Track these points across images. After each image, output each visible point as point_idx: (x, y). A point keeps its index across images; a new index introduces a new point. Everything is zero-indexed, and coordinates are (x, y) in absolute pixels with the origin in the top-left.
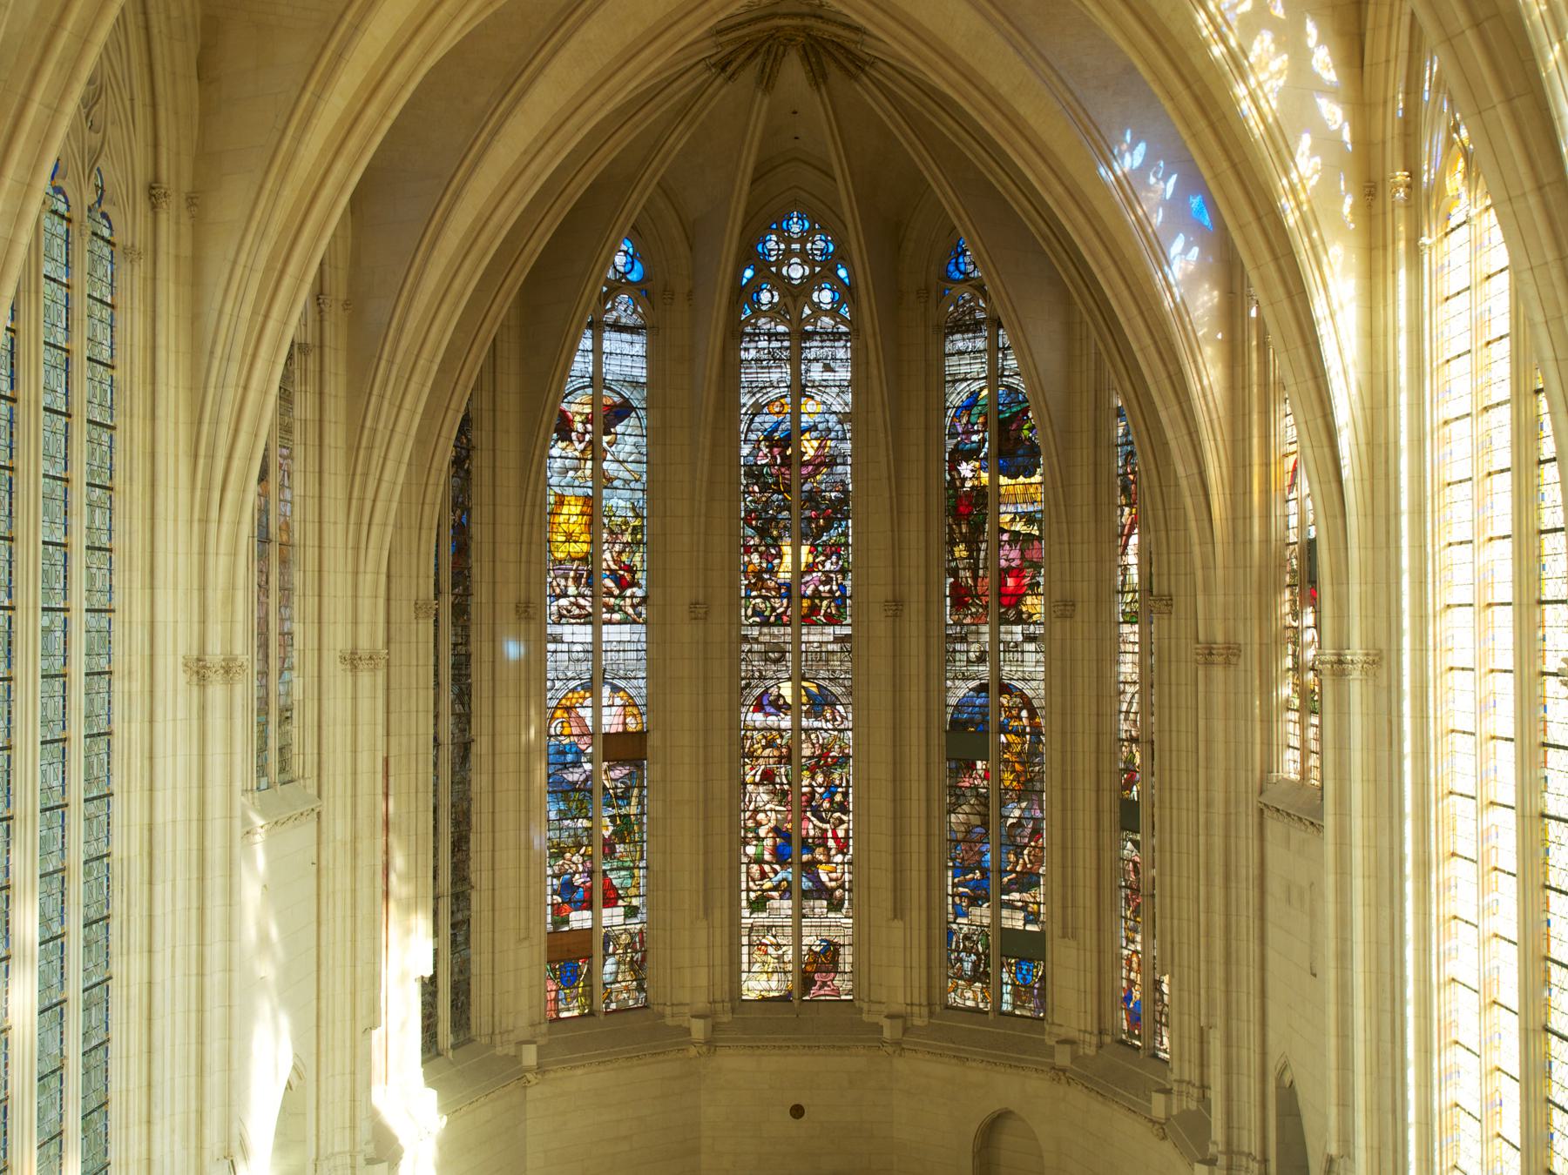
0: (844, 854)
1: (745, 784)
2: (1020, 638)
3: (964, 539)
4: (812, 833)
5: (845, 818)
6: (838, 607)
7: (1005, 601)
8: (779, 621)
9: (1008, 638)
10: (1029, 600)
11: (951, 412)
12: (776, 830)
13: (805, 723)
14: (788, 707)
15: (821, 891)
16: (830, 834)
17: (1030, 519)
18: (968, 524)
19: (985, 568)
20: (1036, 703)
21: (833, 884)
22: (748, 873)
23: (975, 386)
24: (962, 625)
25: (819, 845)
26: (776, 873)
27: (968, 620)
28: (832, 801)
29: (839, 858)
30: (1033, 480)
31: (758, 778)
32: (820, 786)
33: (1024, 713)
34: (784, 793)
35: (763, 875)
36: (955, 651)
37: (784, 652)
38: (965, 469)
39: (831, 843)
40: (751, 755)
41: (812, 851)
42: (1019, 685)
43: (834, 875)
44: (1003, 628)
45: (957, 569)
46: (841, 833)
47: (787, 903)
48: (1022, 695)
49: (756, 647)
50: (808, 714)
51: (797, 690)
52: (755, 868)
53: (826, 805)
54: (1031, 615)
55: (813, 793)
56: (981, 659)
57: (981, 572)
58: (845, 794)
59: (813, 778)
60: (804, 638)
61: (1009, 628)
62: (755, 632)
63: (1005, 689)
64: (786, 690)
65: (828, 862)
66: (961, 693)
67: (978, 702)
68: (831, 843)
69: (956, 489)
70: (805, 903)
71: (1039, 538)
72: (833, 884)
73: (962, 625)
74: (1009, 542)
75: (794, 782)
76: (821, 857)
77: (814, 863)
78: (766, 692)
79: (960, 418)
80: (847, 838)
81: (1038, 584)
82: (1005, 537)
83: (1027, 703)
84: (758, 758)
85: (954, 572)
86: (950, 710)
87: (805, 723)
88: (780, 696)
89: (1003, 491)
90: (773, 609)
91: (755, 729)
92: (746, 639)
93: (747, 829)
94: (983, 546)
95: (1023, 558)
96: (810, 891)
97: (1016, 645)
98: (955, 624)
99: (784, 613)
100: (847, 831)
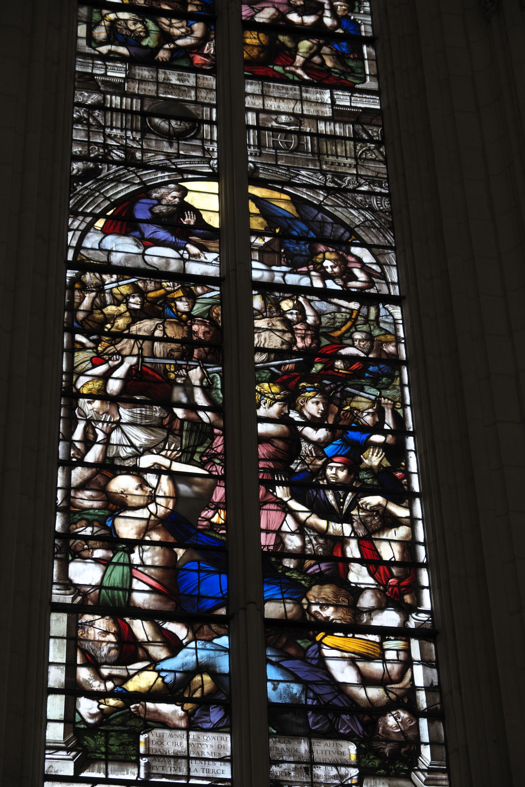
0: (406, 611)
1: (73, 396)
4: (293, 542)
5: (401, 512)
6: (338, 57)
8: (181, 60)
12: (177, 525)
13: (259, 272)
14: (210, 233)
15: (330, 711)
16: (353, 550)
21: (375, 693)
22: (73, 640)
25: (320, 579)
26: (174, 646)
28: (353, 464)
29: (390, 618)
31: (114, 386)
32: (315, 423)
34: (202, 432)
35: (129, 650)
37: (195, 123)
39: (359, 575)
40: (96, 327)
41: (295, 591)
43: (376, 667)
46: (388, 552)
47: (214, 744)
49: (116, 100)
50: (268, 255)
51: (233, 203)
52: (99, 629)
53: (336, 472)
55: (292, 439)
58: (395, 453)
59: (291, 400)
60: (249, 102)
62: (117, 73)
64: (205, 198)
65: (354, 626)
68: (359, 575)
70: (279, 746)
72: (375, 693)
75: (235, 409)
76: (329, 612)
77: (307, 627)
78: (146, 190)
80: (409, 563)
84: (117, 336)
87: (259, 272)
88: (185, 207)
90: (166, 37)
91: (108, 268)
92: (89, 82)
93: (71, 511)
96: (294, 707)
99: (198, 47)
100: (409, 546)
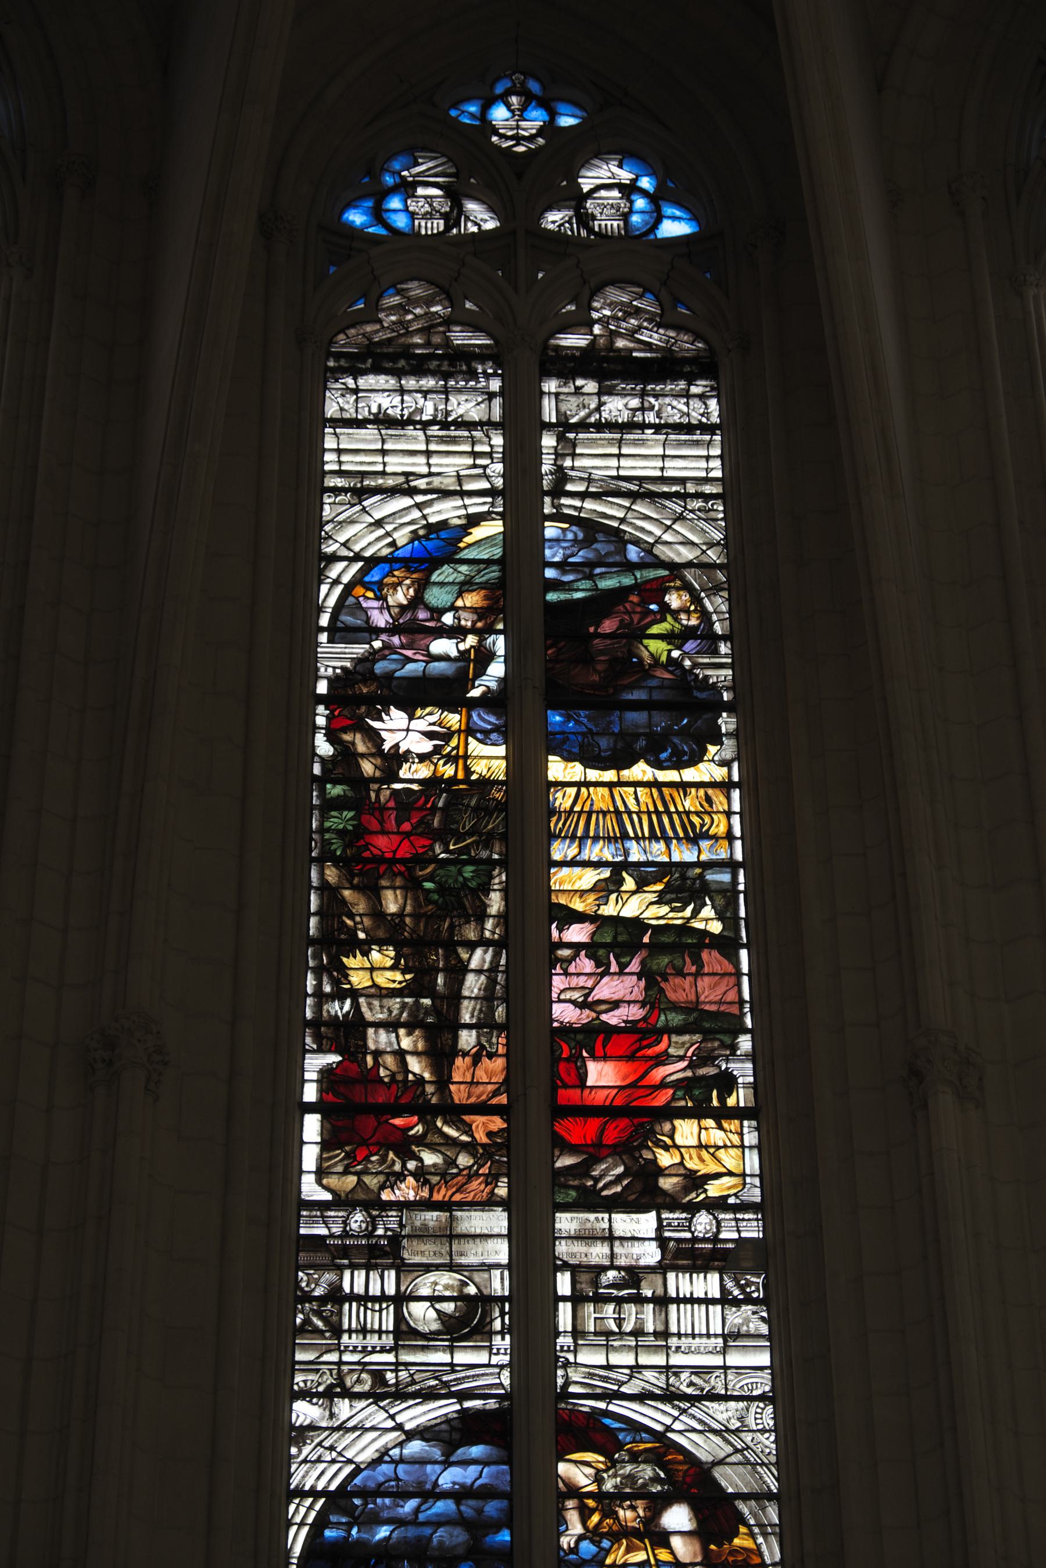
2: (650, 1254)
3: (388, 932)
7: (571, 1129)
9: (598, 1253)
10: (686, 1131)
11: (343, 572)
17: (682, 885)
18: (412, 886)
19: (484, 1024)
20: (730, 1480)
23: (448, 511)
24: (373, 1205)
27: (407, 1190)
30: (690, 775)
33: (677, 1518)
36: (336, 1296)
38: (401, 730)
42: (653, 1416)
44: (566, 1222)
45: (356, 1025)
48: (662, 1449)
54: (696, 1181)
56: (466, 1322)
57: (467, 1039)
61: (598, 1221)
63: (592, 1433)
66: (364, 1449)
67: (449, 1478)
69: (361, 783)
71: (726, 945)
73: (373, 1205)
74: (590, 948)
79: (380, 591)
81: (727, 1083)
82: (577, 933)
83: (692, 1481)
85: (347, 1035)
86: (302, 1512)
89: (563, 800)
94: (479, 958)
95: (654, 998)
97: (634, 1275)
98: (342, 1202)
